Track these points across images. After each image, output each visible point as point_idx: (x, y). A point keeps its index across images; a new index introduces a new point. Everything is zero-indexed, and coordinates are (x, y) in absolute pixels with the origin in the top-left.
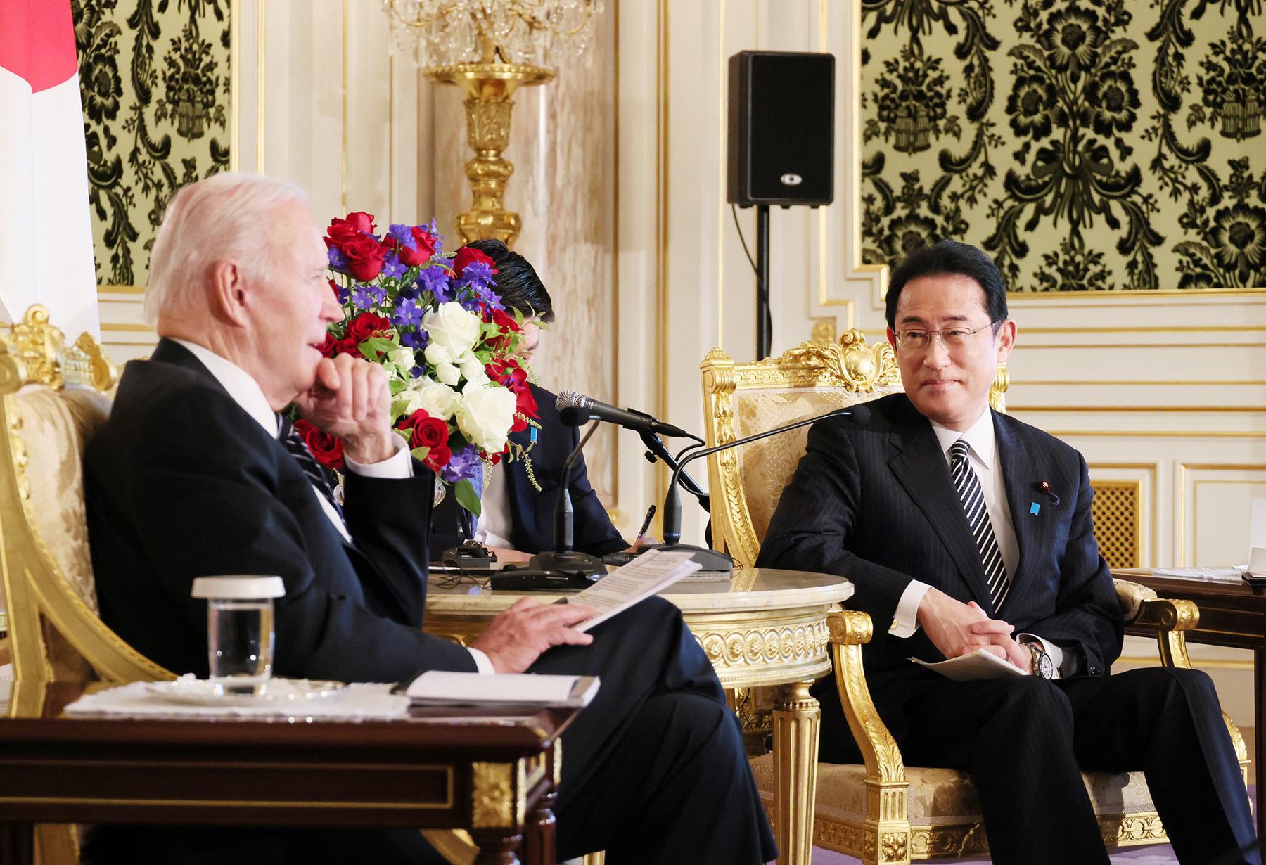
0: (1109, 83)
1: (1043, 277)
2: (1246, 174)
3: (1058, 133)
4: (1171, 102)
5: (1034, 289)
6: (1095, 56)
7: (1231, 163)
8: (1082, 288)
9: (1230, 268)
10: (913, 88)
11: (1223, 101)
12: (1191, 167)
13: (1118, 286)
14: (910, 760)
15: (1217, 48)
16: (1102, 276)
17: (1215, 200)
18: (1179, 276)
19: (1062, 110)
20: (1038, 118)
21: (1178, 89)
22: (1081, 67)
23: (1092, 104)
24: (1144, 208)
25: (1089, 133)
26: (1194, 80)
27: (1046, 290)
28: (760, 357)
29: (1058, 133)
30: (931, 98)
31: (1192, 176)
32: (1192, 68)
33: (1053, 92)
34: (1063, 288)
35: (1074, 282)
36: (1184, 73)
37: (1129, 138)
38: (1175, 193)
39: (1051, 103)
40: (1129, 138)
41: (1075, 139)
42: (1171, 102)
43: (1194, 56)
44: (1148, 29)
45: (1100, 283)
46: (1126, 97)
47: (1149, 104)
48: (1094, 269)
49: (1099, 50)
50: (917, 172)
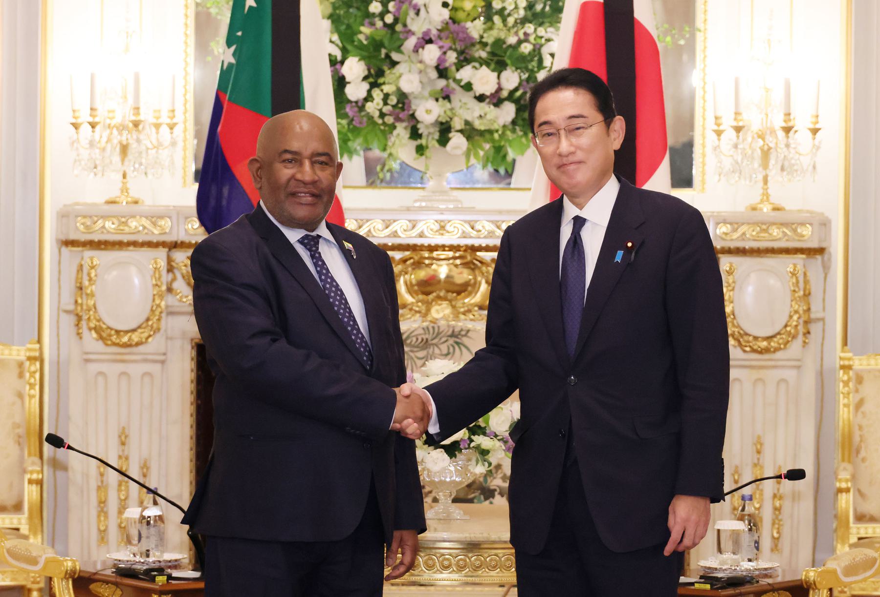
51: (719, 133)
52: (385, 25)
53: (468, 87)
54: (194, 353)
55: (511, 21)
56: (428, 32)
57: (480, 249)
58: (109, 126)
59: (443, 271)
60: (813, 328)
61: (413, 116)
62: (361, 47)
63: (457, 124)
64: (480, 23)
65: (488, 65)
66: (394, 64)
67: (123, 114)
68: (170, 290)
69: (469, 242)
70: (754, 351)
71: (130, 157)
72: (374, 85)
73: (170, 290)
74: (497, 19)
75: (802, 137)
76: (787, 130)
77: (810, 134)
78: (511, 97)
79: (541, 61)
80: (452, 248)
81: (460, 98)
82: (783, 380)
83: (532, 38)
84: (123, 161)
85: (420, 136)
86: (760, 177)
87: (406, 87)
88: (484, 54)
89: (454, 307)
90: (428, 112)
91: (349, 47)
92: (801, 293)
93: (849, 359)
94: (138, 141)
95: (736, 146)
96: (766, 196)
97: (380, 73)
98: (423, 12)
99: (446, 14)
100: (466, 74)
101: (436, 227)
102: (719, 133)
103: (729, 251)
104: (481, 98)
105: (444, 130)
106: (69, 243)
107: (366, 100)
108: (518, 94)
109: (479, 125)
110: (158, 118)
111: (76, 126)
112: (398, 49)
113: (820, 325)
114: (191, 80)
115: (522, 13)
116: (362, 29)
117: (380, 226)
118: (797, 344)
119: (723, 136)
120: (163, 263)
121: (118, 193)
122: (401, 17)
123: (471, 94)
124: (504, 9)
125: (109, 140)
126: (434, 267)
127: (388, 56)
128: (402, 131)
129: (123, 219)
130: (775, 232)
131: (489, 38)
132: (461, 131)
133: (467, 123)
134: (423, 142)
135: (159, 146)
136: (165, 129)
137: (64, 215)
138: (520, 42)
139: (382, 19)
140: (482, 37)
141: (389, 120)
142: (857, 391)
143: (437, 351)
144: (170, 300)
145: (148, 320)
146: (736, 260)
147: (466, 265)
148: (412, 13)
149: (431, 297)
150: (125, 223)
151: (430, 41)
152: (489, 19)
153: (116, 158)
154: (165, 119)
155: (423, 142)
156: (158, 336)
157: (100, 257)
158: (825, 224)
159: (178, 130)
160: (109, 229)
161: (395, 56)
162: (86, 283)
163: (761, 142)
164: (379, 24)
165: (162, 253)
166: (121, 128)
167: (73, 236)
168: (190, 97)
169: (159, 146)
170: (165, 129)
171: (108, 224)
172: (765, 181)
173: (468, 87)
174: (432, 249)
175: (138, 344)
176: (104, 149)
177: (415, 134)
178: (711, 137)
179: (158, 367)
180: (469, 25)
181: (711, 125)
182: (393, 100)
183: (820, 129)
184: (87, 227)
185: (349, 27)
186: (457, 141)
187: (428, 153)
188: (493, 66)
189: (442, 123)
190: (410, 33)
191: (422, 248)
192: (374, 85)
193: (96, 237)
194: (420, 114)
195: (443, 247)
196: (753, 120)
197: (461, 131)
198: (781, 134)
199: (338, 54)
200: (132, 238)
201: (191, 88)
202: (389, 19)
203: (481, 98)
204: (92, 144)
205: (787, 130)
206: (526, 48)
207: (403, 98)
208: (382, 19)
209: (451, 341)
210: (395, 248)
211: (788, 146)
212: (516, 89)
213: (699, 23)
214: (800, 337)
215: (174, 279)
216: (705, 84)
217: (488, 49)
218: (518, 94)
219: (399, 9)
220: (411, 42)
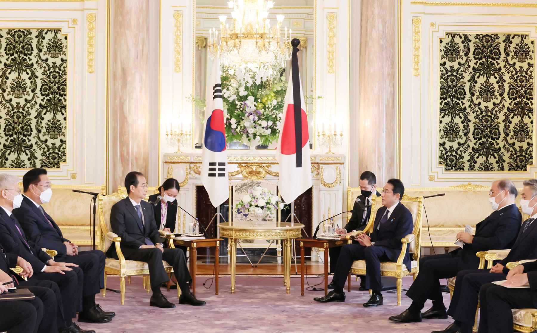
0: (26, 127)
1: (11, 165)
2: (55, 146)
3: (15, 136)
4: (39, 131)
5: (10, 167)
6: (23, 121)
7: (52, 144)
8: (20, 167)
9: (51, 164)
10: (54, 126)
11: (50, 131)
12: (43, 144)
13: (28, 167)
14: (126, 259)
15: (49, 121)
16: (24, 165)
17: (48, 151)
18: (41, 165)
19: (16, 132)
20: (10, 133)
21: (41, 129)
22: (20, 123)
23: (22, 131)
24: (33, 152)
25: (22, 136)
26: (44, 127)
27: (12, 168)
28: (200, 179)
29: (15, 136)
30: (58, 128)
31: (44, 146)
32: (44, 124)
33: (14, 128)
34: (16, 167)
35: (18, 166)
36: (42, 125)
37: (30, 138)
38: (40, 149)
39: (13, 130)
40: (30, 138)
41: (19, 138)
42: (39, 131)
43: (44, 122)
44: (35, 117)
45: (24, 166)
46: (30, 130)
47: (35, 132)
48: (23, 164)
49: (24, 120)
50: (55, 143)
51: (319, 136)
52: (240, 110)
53: (260, 125)
54: (196, 189)
55: (270, 110)
56: (250, 112)
57: (263, 163)
58: (175, 135)
59: (254, 169)
60: (341, 181)
61: (247, 132)
62: (235, 116)
63: (258, 134)
64: (263, 110)
65: (265, 120)
66: (243, 120)
67: (178, 132)
68: (190, 173)
69: (261, 162)
70: (328, 187)
71: (180, 142)
72: (238, 125)
73: (190, 173)
74: (267, 109)
75: (338, 136)
76: (335, 135)
77: (340, 136)
78: (270, 128)
79: (277, 119)
80: (256, 163)
81: (258, 127)
82: (335, 194)
83: (275, 114)
84: (178, 143)
85: (249, 137)
86: (329, 146)
87: (246, 125)
88: (264, 118)
89: (257, 177)
90: (251, 131)
91: (232, 116)
92: (339, 173)
93: (350, 189)
94: (182, 138)
95: (323, 139)
96: (330, 151)
97: (240, 122)
98: (249, 107)
99: (255, 108)
100: (260, 122)
101: (253, 158)
102: (319, 136)
103: (322, 164)
104: (263, 128)
105: (255, 135)
106: (166, 162)
107: (236, 128)
108: (272, 127)
109: (263, 134)
110: (186, 133)
111: (167, 135)
112: (244, 116)
113: (343, 180)
114: (194, 124)
115: (273, 108)
116: (235, 111)
117: (239, 158)
118: (338, 185)
119: (320, 137)
120: (188, 167)
121: (177, 151)
122: (244, 109)
123: (261, 127)
124: (268, 107)
125: (175, 138)
126: (252, 168)
127: (241, 118)
128: (245, 136)
129: (178, 156)
130: (333, 159)
131: (265, 114)
132: (259, 135)
133: (260, 134)
134: (250, 138)
135: (187, 140)
136: (188, 136)
137: (165, 156)
138: (272, 114)
139: (240, 109)
140: (263, 113)
141: (242, 133)
142: (352, 196)
143: (253, 187)
144: (190, 176)
145: (185, 180)
146: (324, 166)
147: (260, 167)
148: (247, 108)
149: (252, 175)
150: (179, 158)
151: (251, 114)
152: (265, 109)
153: (177, 143)
154: (188, 133)
155: (250, 138)
156: (187, 184)
157: (173, 166)
158: (344, 157)
159: (191, 136)
160: (176, 159)
161: (243, 118)
162: (170, 172)
163: (329, 138)
164: (239, 110)
165: (188, 165)
166: (178, 135)
167: (167, 161)
168: (194, 128)
169: (187, 140)
170: (188, 136)
171: (175, 158)
172: (330, 146)
173: (260, 125)
174: (252, 163)
175: (183, 186)
176: (174, 140)
177: (248, 136)
178: (317, 137)
179: (187, 191)
180: (260, 110)
181: (317, 134)
182: (243, 128)
183: (342, 135)
184: (170, 159)
185: (232, 111)
186: (258, 138)
187: (251, 141)
188: (266, 120)
189: (254, 134)
190: (247, 112)
191: (249, 163)
192: (238, 125)
193: (172, 161)
194: (249, 131)
195: (254, 163)
196: (327, 133)
197: (259, 135)
198: (333, 136)
199: (229, 117)
200: (181, 161)
201: (194, 126)
202: (241, 109)
203: (263, 128)
204: (171, 139)
205: (335, 135)
206: (274, 116)
207: (245, 128)
208: (240, 109)
209: (257, 185)
210: (243, 163)
211: (335, 139)
212: (271, 126)
213: (314, 110)
214: (339, 184)
215: (191, 171)
216: (315, 125)
217: (265, 116)
218: (272, 127)
219: (244, 107)
220: (247, 115)
